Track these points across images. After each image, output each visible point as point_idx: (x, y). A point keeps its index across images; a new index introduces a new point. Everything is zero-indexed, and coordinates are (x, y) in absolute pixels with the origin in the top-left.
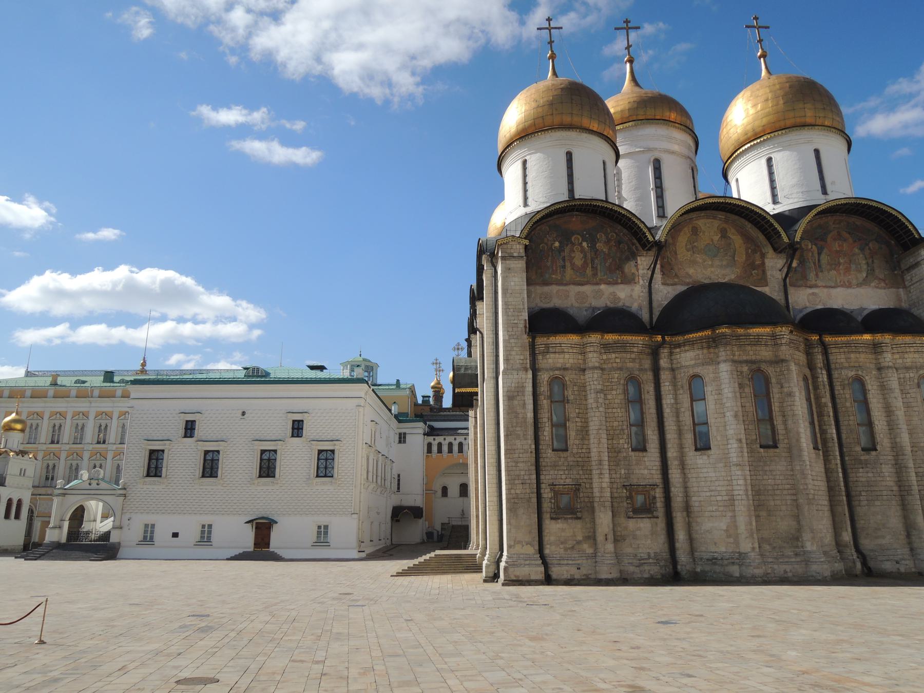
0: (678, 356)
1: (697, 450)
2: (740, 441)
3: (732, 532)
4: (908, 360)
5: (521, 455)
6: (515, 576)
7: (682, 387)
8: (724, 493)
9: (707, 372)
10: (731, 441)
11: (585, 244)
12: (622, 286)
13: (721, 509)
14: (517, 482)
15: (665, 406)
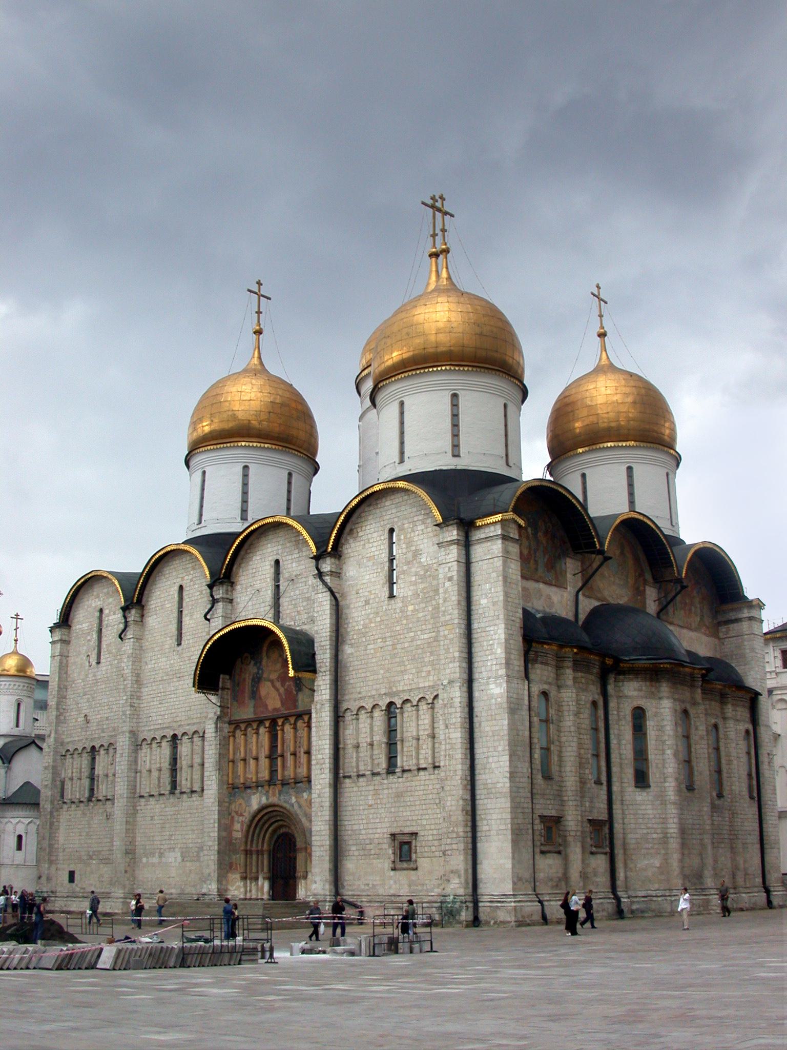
0: (621, 684)
1: (636, 787)
2: (677, 779)
3: (664, 869)
4: (739, 713)
5: (521, 780)
6: (523, 916)
7: (625, 718)
8: (659, 831)
9: (649, 706)
10: (670, 779)
11: (529, 530)
12: (554, 589)
13: (656, 846)
14: (519, 810)
15: (612, 737)
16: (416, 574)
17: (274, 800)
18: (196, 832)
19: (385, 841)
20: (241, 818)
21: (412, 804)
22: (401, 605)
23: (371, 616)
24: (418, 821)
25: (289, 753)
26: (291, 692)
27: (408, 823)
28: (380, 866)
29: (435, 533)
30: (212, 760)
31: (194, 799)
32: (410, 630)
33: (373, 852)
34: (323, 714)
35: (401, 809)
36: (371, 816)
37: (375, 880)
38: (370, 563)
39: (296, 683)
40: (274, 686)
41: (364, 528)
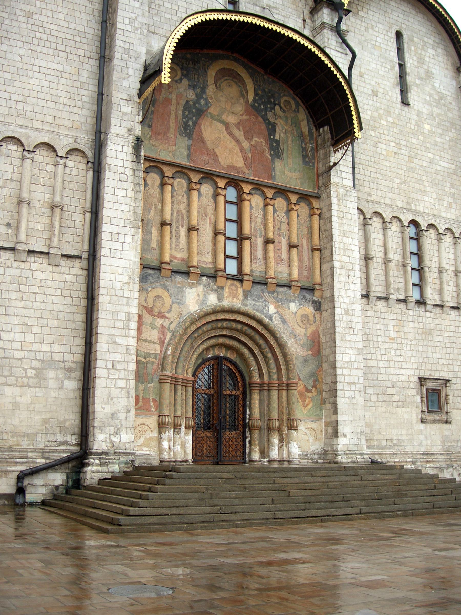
16: (430, 96)
17: (237, 304)
18: (35, 330)
19: (412, 385)
20: (159, 322)
21: (443, 345)
22: (416, 117)
23: (381, 112)
24: (450, 366)
25: (260, 241)
26: (262, 154)
27: (439, 367)
28: (406, 416)
29: (446, 66)
30: (124, 208)
31: (35, 266)
32: (427, 150)
33: (396, 398)
34: (349, 204)
35: (430, 349)
36: (393, 352)
37: (401, 435)
38: (377, 53)
39: (271, 145)
40: (231, 134)
41: (365, 10)
